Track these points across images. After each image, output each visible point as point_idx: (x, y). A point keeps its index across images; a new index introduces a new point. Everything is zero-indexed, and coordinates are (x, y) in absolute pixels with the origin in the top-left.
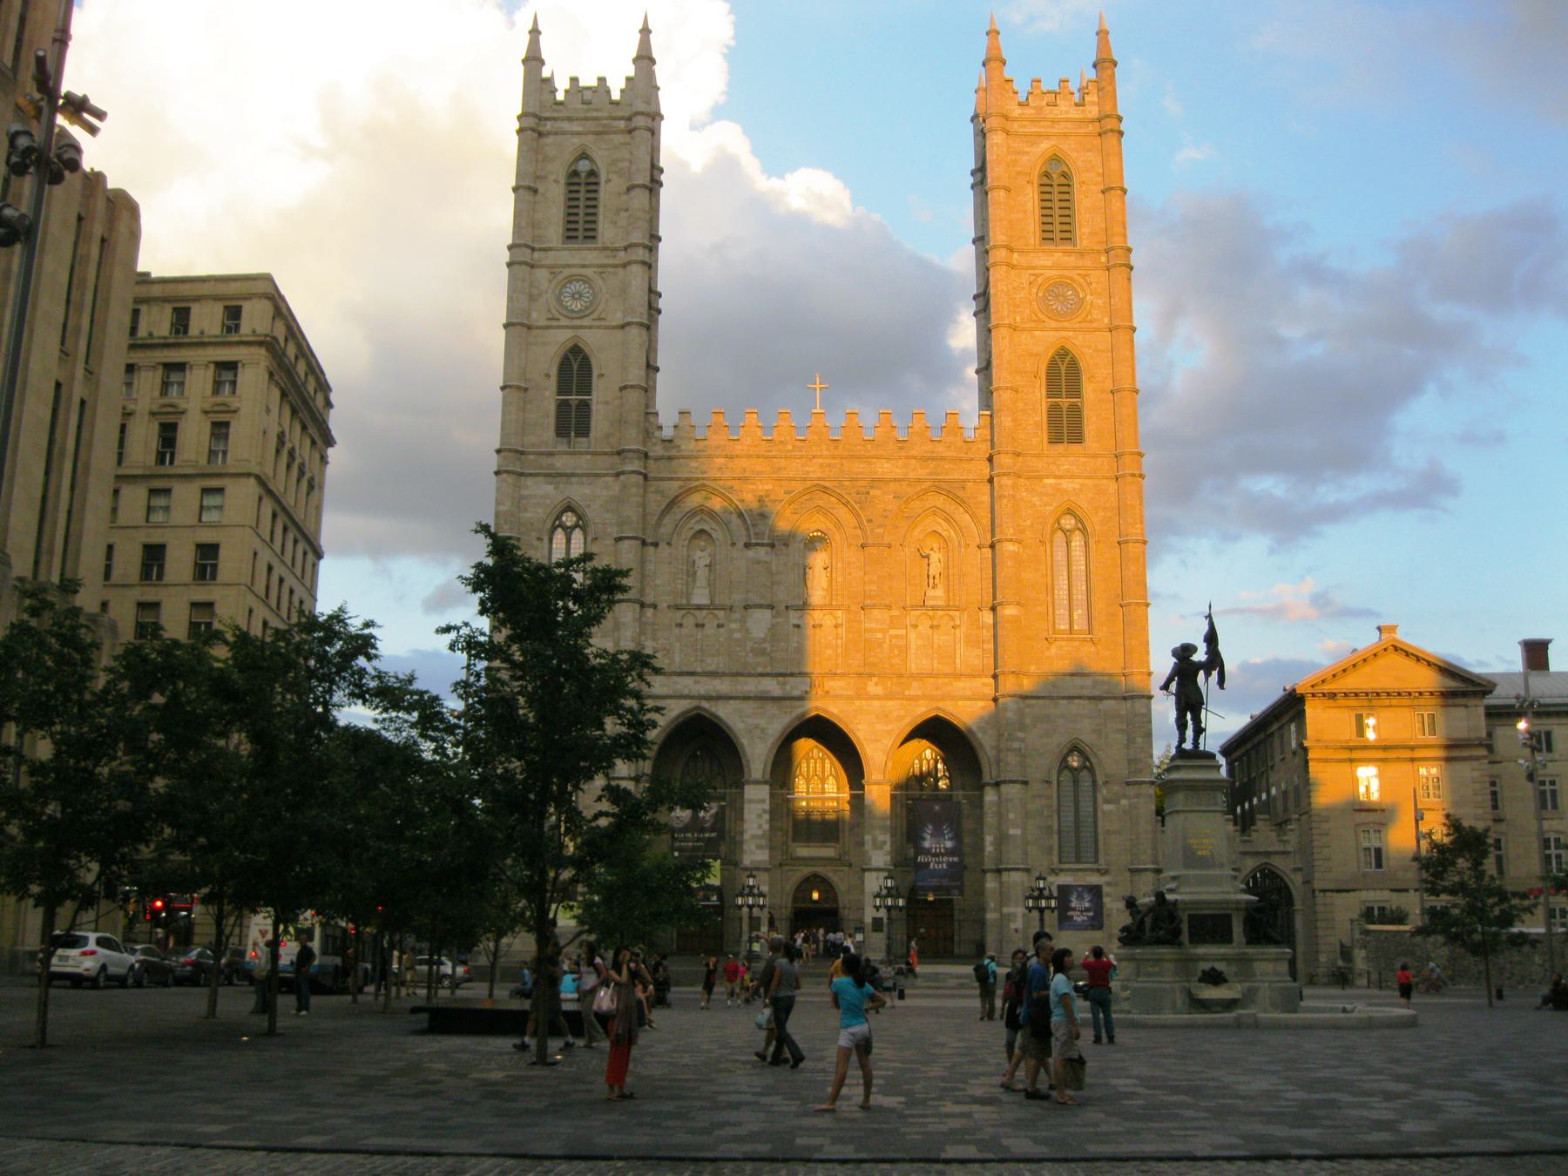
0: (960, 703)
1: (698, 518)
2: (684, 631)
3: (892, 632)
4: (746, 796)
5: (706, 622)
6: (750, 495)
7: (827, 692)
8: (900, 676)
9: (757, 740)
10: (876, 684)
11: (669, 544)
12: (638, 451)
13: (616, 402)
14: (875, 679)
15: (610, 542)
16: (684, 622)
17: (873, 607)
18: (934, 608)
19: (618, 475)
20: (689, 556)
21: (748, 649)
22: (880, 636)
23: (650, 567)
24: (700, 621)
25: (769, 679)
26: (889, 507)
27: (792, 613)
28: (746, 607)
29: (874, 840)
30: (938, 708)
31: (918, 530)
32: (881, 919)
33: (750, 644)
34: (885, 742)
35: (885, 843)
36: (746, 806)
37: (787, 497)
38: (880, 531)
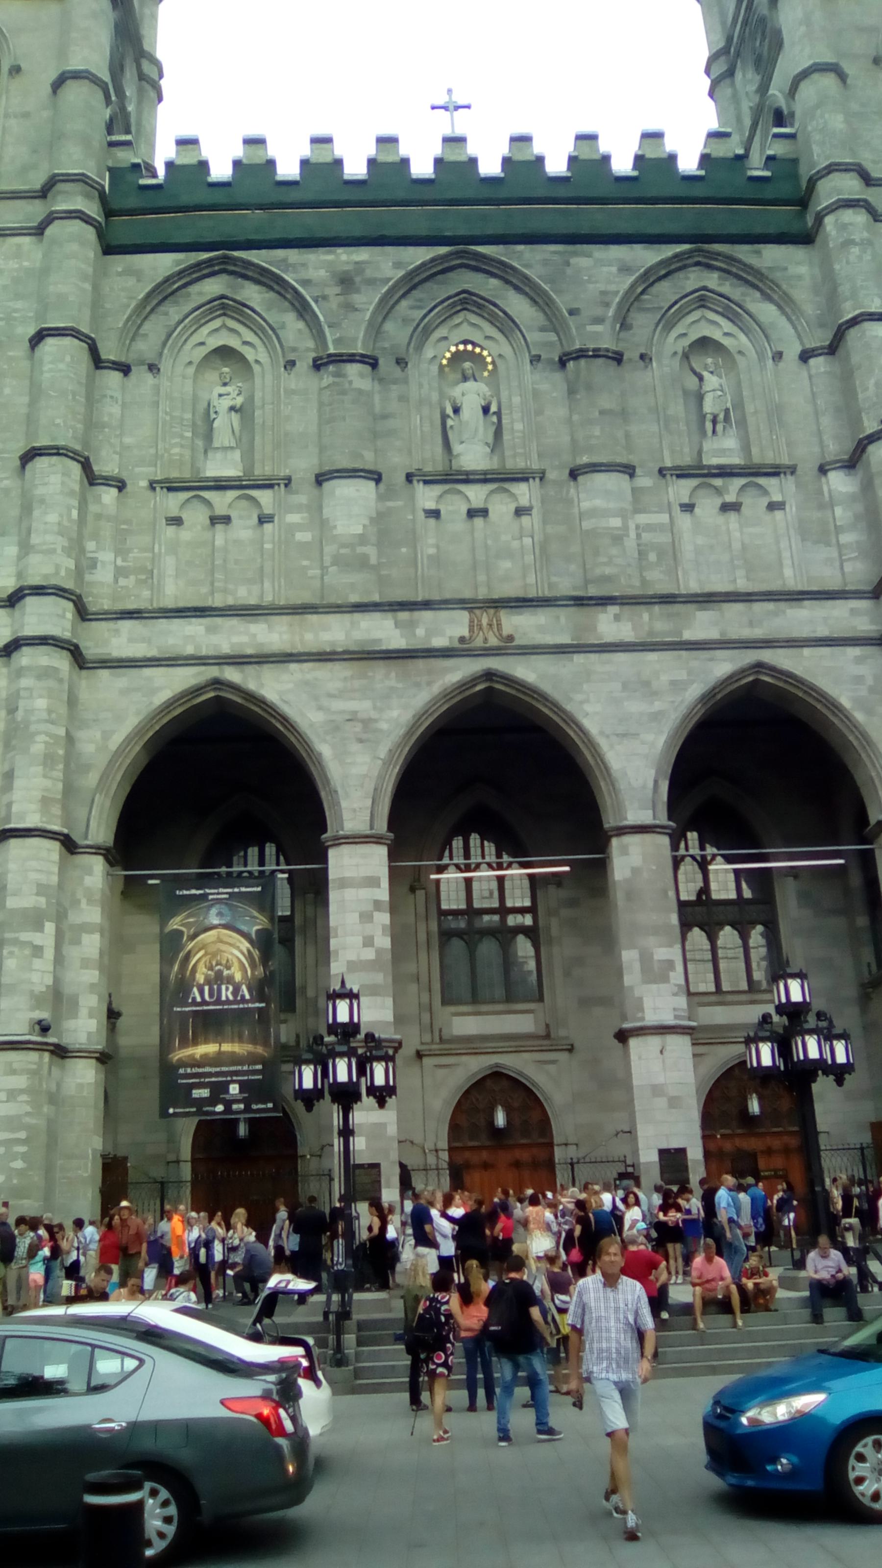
0: (806, 651)
1: (217, 323)
2: (185, 534)
3: (643, 519)
4: (332, 875)
5: (234, 515)
6: (322, 273)
7: (510, 638)
8: (668, 599)
9: (355, 747)
10: (617, 618)
11: (153, 368)
12: (82, 179)
13: (45, 114)
14: (613, 610)
15: (20, 351)
16: (184, 516)
17: (595, 468)
18: (725, 472)
19: (39, 231)
20: (195, 399)
21: (327, 560)
22: (616, 522)
23: (111, 411)
24: (220, 511)
25: (377, 615)
26: (612, 288)
27: (420, 488)
28: (320, 479)
29: (646, 958)
30: (759, 666)
31: (674, 334)
32: (682, 1152)
33: (330, 550)
34: (649, 737)
35: (670, 964)
36: (334, 896)
37: (401, 273)
38: (599, 328)
